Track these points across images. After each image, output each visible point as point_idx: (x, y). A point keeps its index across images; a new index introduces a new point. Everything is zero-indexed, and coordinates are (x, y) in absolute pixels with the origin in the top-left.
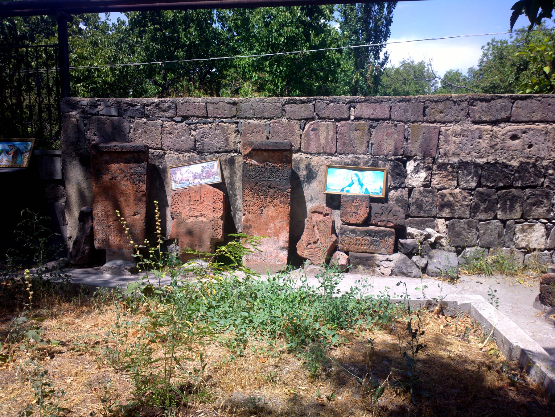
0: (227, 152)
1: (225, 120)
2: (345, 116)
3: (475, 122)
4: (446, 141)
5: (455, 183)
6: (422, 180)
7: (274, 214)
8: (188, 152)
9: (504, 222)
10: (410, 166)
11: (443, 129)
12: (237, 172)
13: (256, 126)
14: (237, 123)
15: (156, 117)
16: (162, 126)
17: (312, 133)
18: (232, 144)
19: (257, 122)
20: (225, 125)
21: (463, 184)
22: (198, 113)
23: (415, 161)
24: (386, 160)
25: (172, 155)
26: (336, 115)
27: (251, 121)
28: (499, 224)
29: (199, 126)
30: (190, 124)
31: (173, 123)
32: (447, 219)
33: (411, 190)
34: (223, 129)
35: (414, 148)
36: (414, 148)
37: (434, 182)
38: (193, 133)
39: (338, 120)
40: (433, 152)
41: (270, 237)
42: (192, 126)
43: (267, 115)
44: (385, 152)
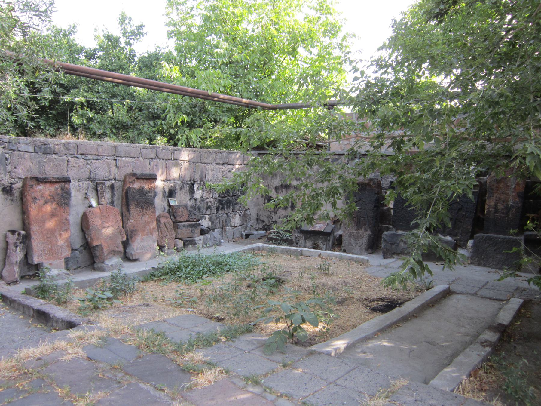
0: (109, 180)
1: (108, 158)
2: (170, 158)
3: (217, 164)
4: (208, 174)
5: (211, 195)
6: (200, 194)
7: (149, 220)
8: (85, 180)
9: (227, 214)
10: (196, 187)
11: (207, 167)
12: (116, 194)
13: (127, 162)
14: (116, 160)
15: (63, 154)
16: (68, 161)
17: (155, 167)
18: (112, 174)
19: (127, 159)
20: (108, 161)
21: (214, 196)
22: (92, 153)
23: (197, 184)
24: (187, 184)
25: (74, 183)
26: (165, 157)
27: (124, 159)
28: (225, 215)
29: (93, 161)
30: (86, 160)
31: (75, 159)
32: (209, 215)
33: (196, 200)
34: (108, 163)
35: (197, 177)
36: (197, 177)
37: (204, 195)
38: (89, 166)
39: (166, 160)
40: (204, 179)
41: (148, 235)
42: (89, 162)
43: (132, 155)
44: (186, 179)
